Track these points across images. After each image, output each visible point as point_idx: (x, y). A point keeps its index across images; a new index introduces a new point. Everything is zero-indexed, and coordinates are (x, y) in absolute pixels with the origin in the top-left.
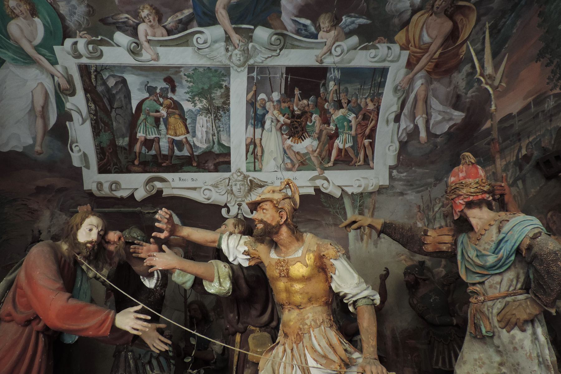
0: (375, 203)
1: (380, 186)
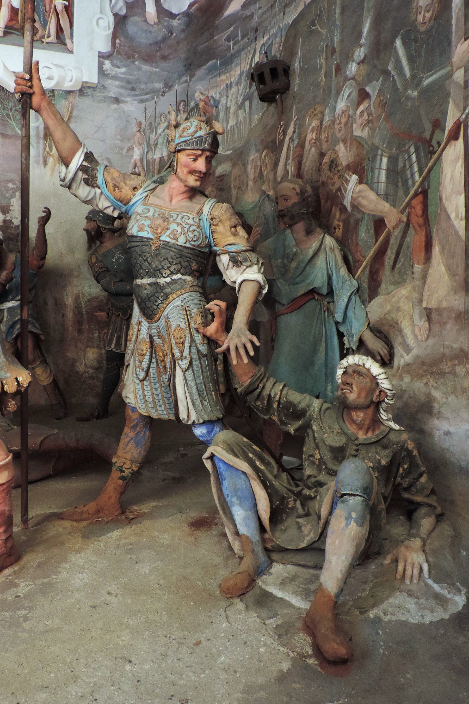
0: (72, 109)
1: (83, 82)
